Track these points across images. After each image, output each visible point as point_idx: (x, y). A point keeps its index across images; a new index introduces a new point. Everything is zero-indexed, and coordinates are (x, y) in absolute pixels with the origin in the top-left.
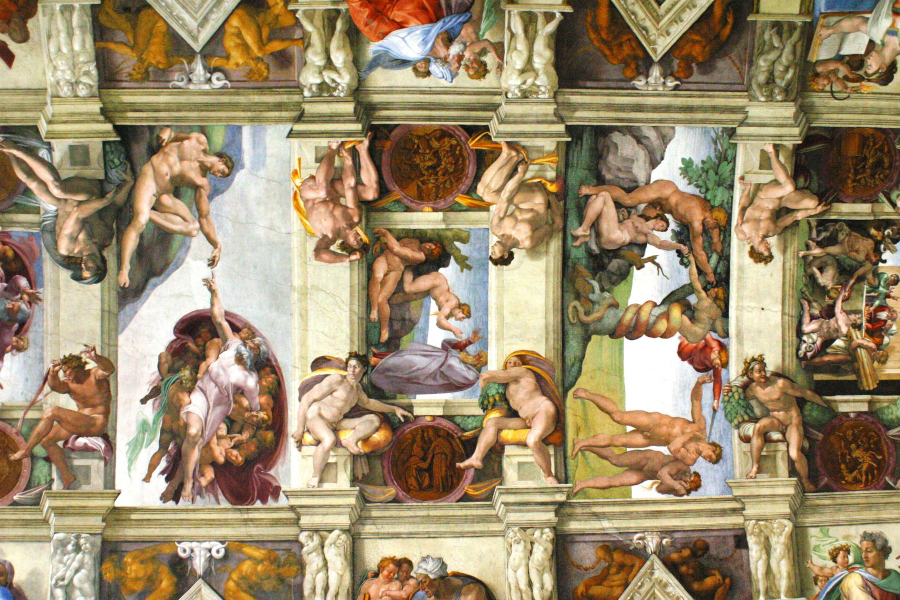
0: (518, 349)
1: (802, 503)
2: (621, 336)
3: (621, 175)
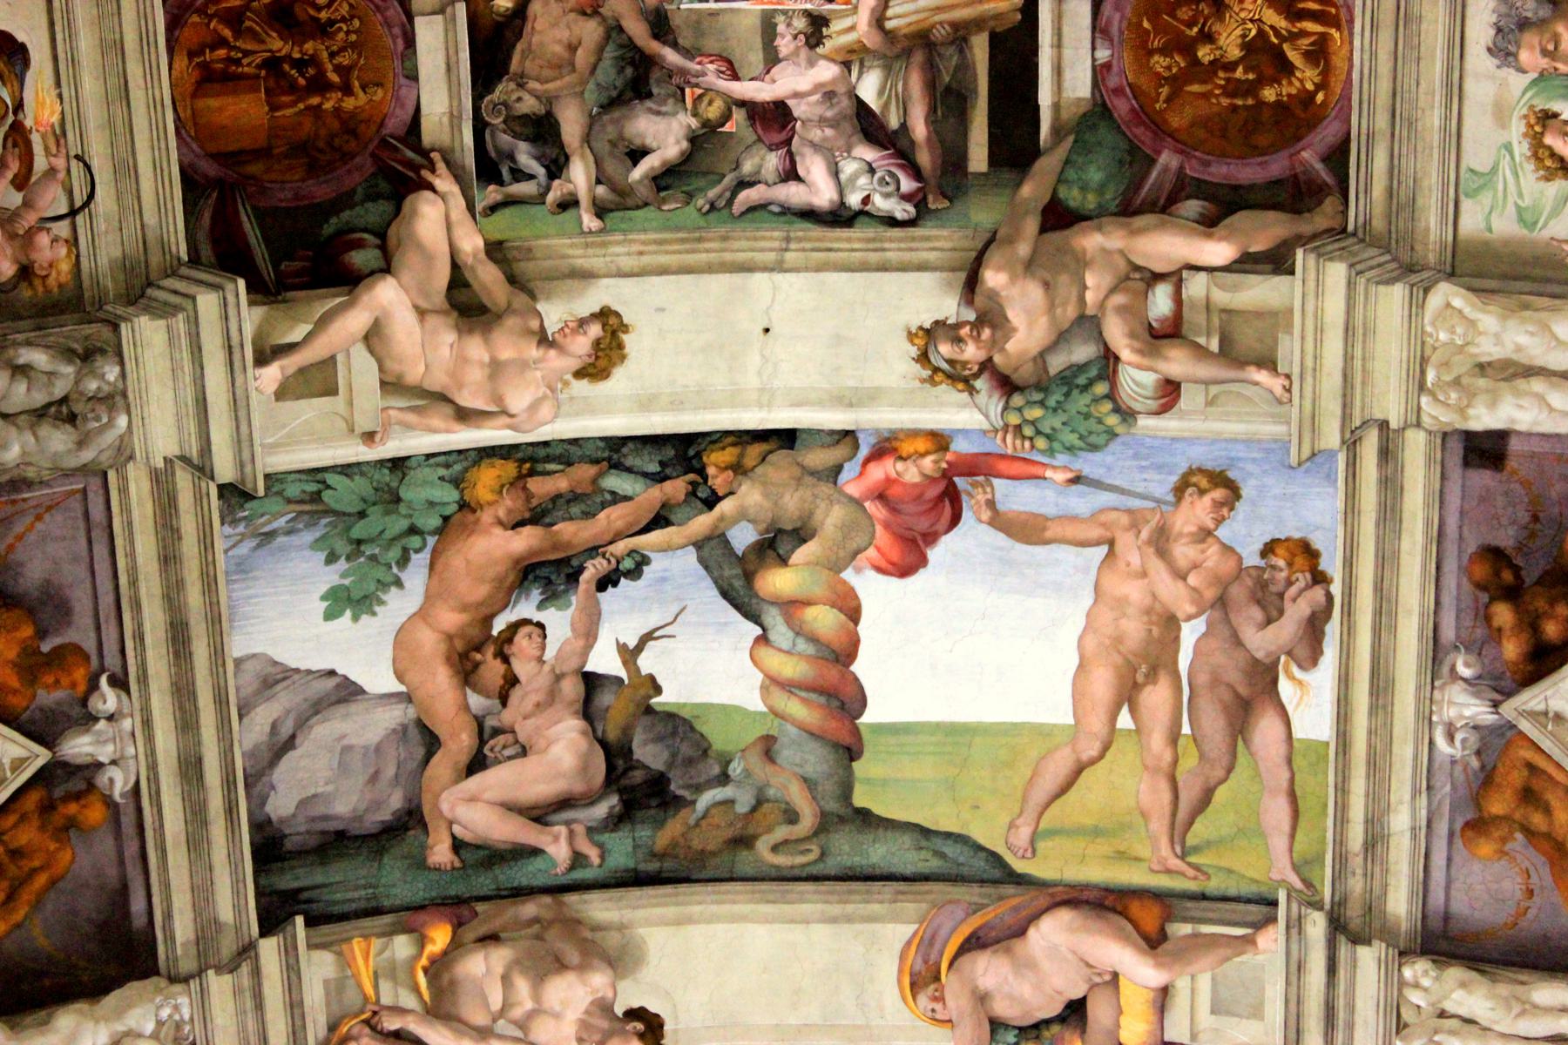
0: (896, 991)
1: (1383, 244)
2: (856, 732)
3: (390, 771)
